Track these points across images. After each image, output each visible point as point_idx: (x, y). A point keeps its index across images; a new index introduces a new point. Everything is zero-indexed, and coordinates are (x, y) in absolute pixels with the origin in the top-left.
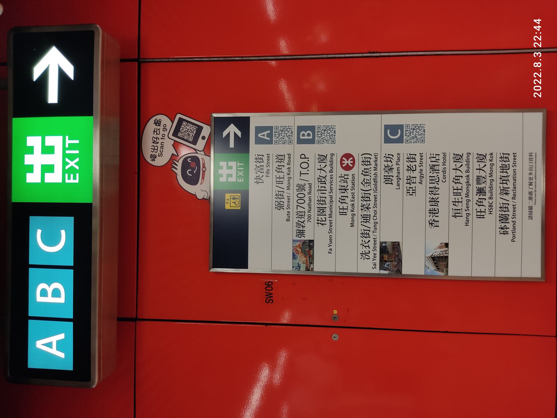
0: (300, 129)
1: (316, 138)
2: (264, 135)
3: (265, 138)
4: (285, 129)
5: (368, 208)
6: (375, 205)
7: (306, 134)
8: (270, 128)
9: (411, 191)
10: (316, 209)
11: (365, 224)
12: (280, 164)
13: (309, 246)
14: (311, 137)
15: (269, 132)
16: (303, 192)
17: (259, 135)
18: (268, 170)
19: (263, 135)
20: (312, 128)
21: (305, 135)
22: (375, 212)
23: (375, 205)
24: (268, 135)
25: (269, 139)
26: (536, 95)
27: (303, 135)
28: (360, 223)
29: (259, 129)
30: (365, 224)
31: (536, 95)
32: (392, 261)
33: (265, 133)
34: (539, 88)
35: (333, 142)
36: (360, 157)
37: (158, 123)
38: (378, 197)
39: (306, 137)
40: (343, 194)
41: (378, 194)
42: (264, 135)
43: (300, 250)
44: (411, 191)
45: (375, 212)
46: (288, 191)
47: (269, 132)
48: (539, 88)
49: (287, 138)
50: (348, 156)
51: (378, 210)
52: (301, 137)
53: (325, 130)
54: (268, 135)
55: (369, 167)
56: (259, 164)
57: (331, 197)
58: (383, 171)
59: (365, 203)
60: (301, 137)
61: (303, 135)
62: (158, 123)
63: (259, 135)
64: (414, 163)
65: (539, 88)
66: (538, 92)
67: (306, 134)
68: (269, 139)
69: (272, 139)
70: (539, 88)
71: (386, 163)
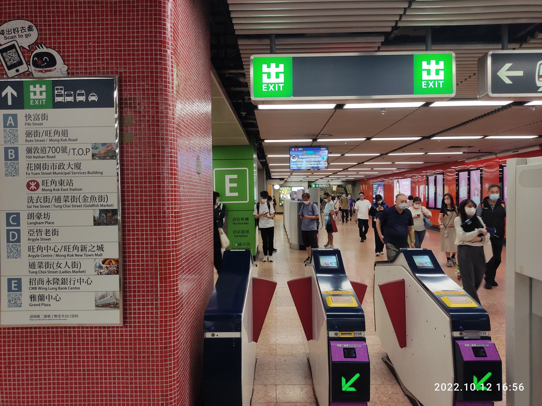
0: (16, 149)
1: (9, 162)
2: (10, 121)
3: (9, 122)
4: (16, 137)
5: (66, 201)
6: (74, 206)
7: (12, 154)
8: (16, 126)
9: (31, 232)
10: (39, 162)
11: (54, 199)
12: (61, 133)
13: (113, 156)
14: (10, 158)
15: (13, 125)
16: (61, 152)
17: (10, 117)
18: (30, 124)
19: (10, 121)
20: (16, 158)
21: (11, 153)
22: (69, 206)
23: (74, 206)
24: (10, 124)
25: (8, 125)
27: (11, 152)
28: (54, 195)
29: (15, 117)
30: (54, 199)
32: (106, 219)
33: (12, 122)
34: (444, 388)
35: (6, 175)
36: (105, 194)
37: (30, 29)
38: (81, 208)
39: (10, 154)
40: (58, 183)
41: (83, 208)
42: (10, 121)
43: (109, 149)
44: (31, 232)
45: (69, 206)
46: (48, 140)
47: (13, 125)
48: (444, 389)
49: (8, 139)
50: (28, 186)
51: (71, 208)
52: (9, 150)
53: (15, 168)
54: (10, 124)
55: (97, 200)
56: (40, 117)
57: (69, 173)
58: (37, 212)
59: (70, 198)
60: (9, 150)
61: (11, 152)
62: (30, 29)
63: (10, 117)
64: (51, 234)
65: (444, 388)
66: (440, 388)
67: (12, 154)
68: (8, 125)
69: (8, 127)
70: (444, 389)
71: (43, 214)
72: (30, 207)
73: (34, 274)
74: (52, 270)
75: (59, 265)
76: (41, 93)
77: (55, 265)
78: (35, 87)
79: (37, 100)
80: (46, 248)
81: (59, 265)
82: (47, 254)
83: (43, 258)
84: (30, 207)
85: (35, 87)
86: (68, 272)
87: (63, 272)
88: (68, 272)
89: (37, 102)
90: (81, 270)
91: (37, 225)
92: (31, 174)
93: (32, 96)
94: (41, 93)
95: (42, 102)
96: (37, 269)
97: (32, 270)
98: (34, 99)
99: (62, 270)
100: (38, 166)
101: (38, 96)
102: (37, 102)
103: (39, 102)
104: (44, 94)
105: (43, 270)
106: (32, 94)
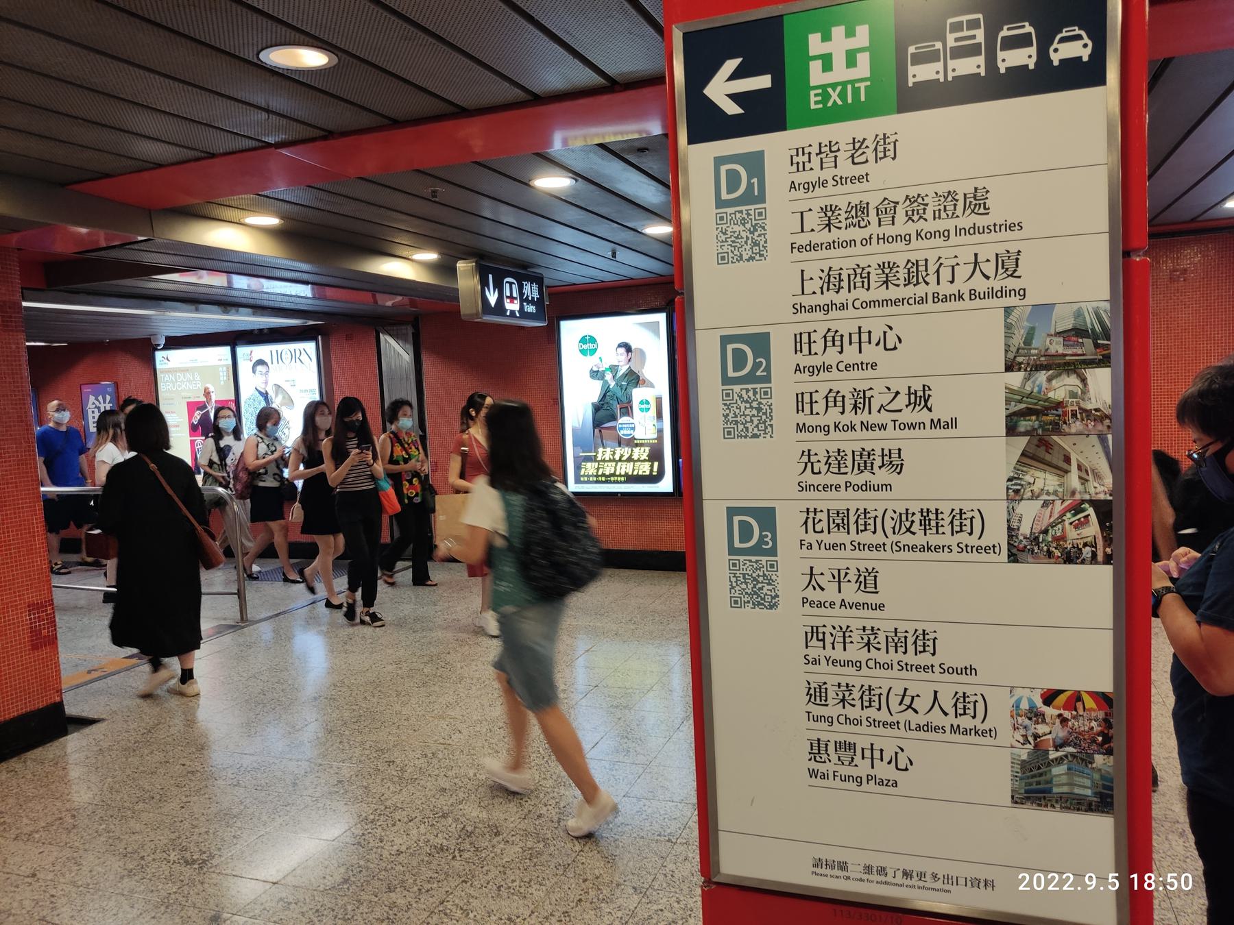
26: (1024, 878)
29: (755, 163)
31: (1024, 878)
72: (816, 662)
73: (824, 725)
74: (883, 715)
75: (907, 701)
76: (851, 61)
77: (894, 701)
78: (826, 37)
79: (834, 86)
80: (855, 338)
81: (907, 701)
82: (858, 359)
83: (845, 375)
84: (816, 662)
85: (826, 37)
86: (936, 729)
87: (919, 728)
88: (936, 729)
89: (835, 96)
90: (981, 727)
91: (834, 314)
92: (815, 546)
93: (817, 76)
94: (851, 61)
95: (856, 91)
96: (833, 710)
97: (818, 711)
98: (824, 87)
99: (915, 719)
100: (840, 521)
101: (841, 73)
102: (835, 96)
103: (843, 95)
104: (864, 60)
105: (853, 713)
106: (815, 67)
